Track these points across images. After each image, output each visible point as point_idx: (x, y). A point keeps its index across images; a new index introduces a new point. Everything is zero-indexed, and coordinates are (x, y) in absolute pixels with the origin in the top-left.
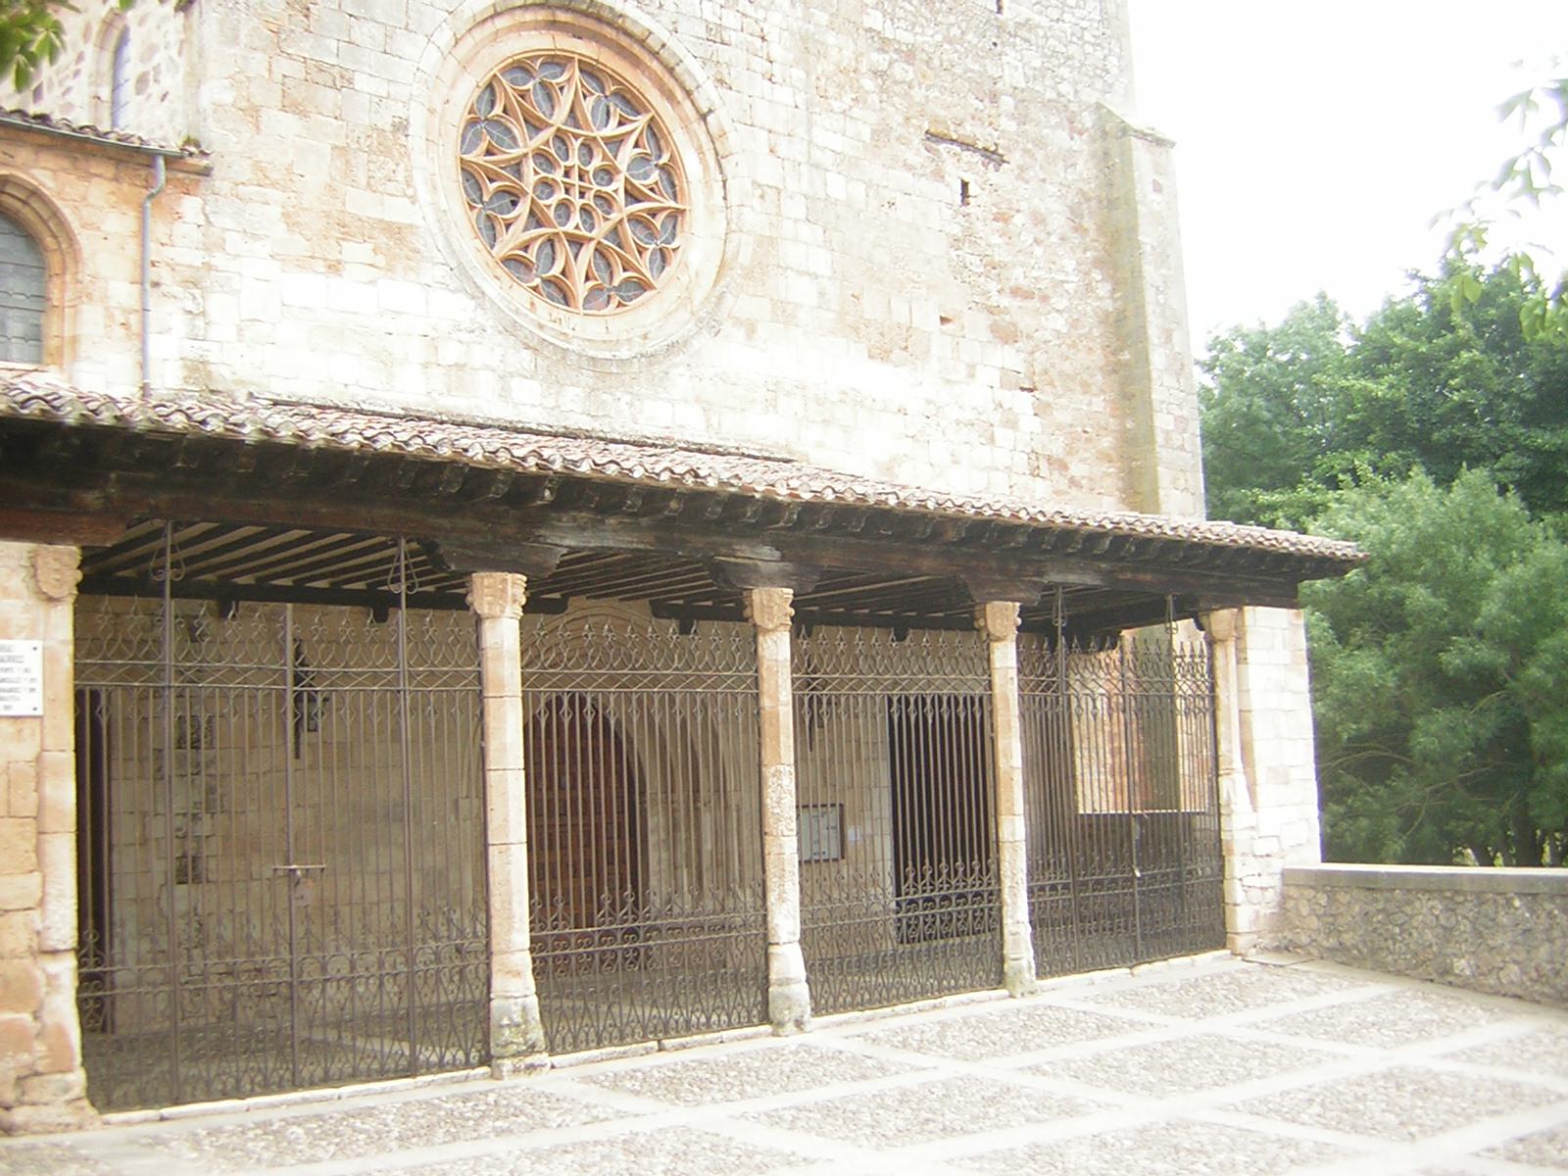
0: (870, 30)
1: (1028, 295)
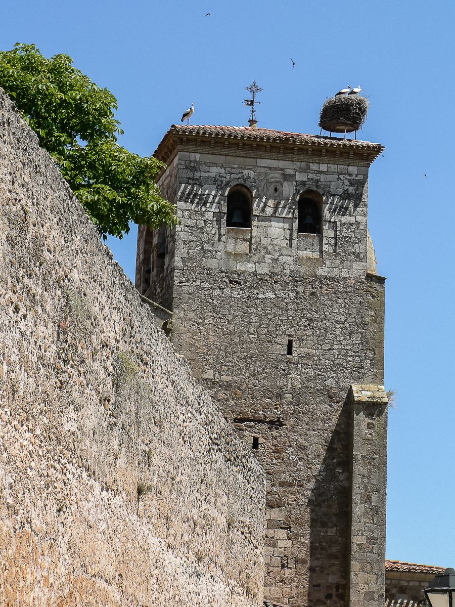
0: (205, 380)
1: (290, 485)
